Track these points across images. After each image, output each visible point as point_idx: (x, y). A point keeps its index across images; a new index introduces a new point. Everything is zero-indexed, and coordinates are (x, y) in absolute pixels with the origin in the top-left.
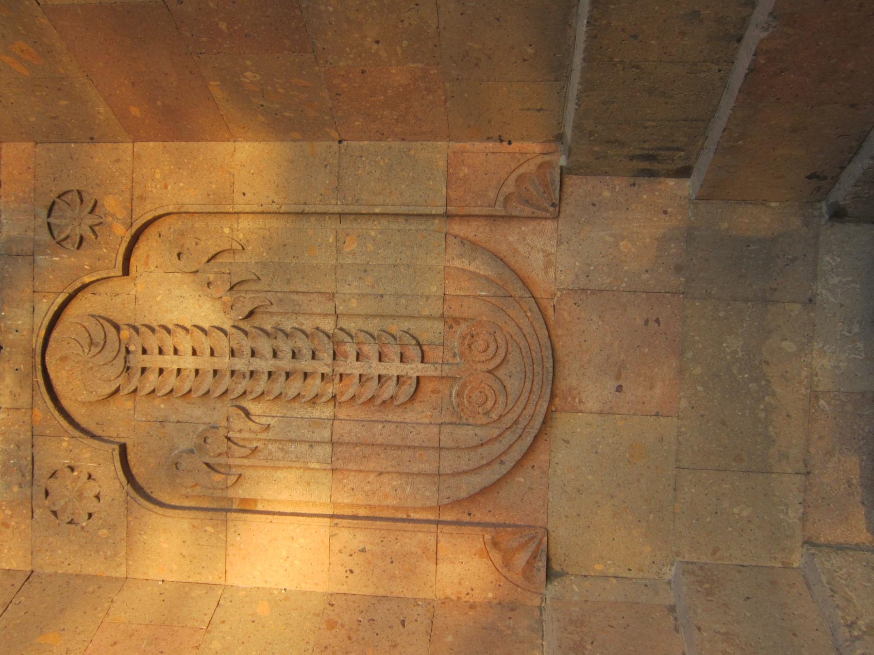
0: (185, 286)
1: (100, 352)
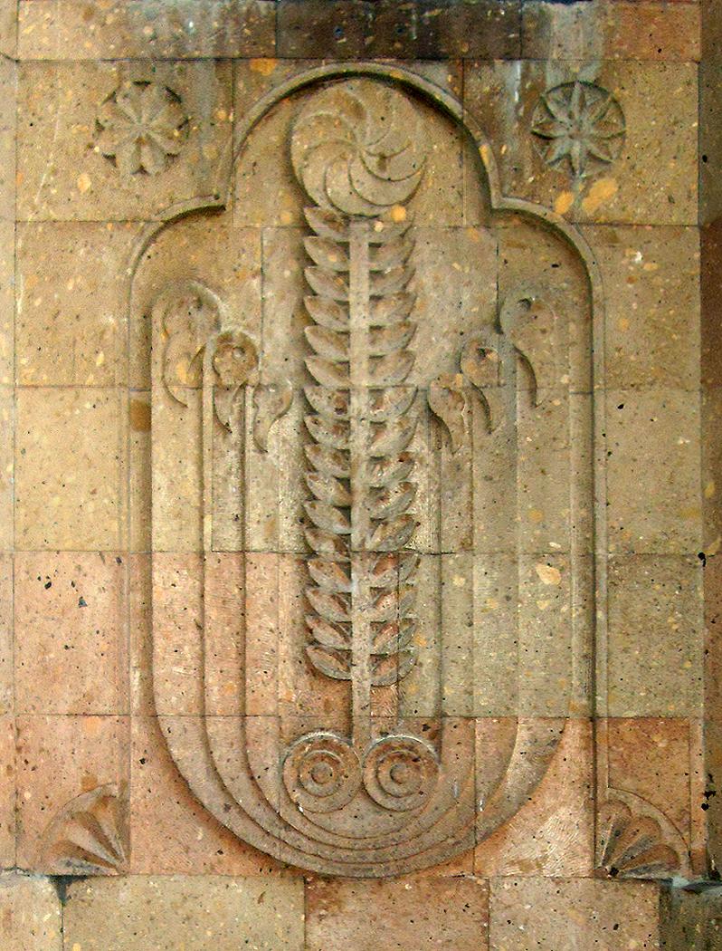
0: (476, 309)
1: (369, 172)
